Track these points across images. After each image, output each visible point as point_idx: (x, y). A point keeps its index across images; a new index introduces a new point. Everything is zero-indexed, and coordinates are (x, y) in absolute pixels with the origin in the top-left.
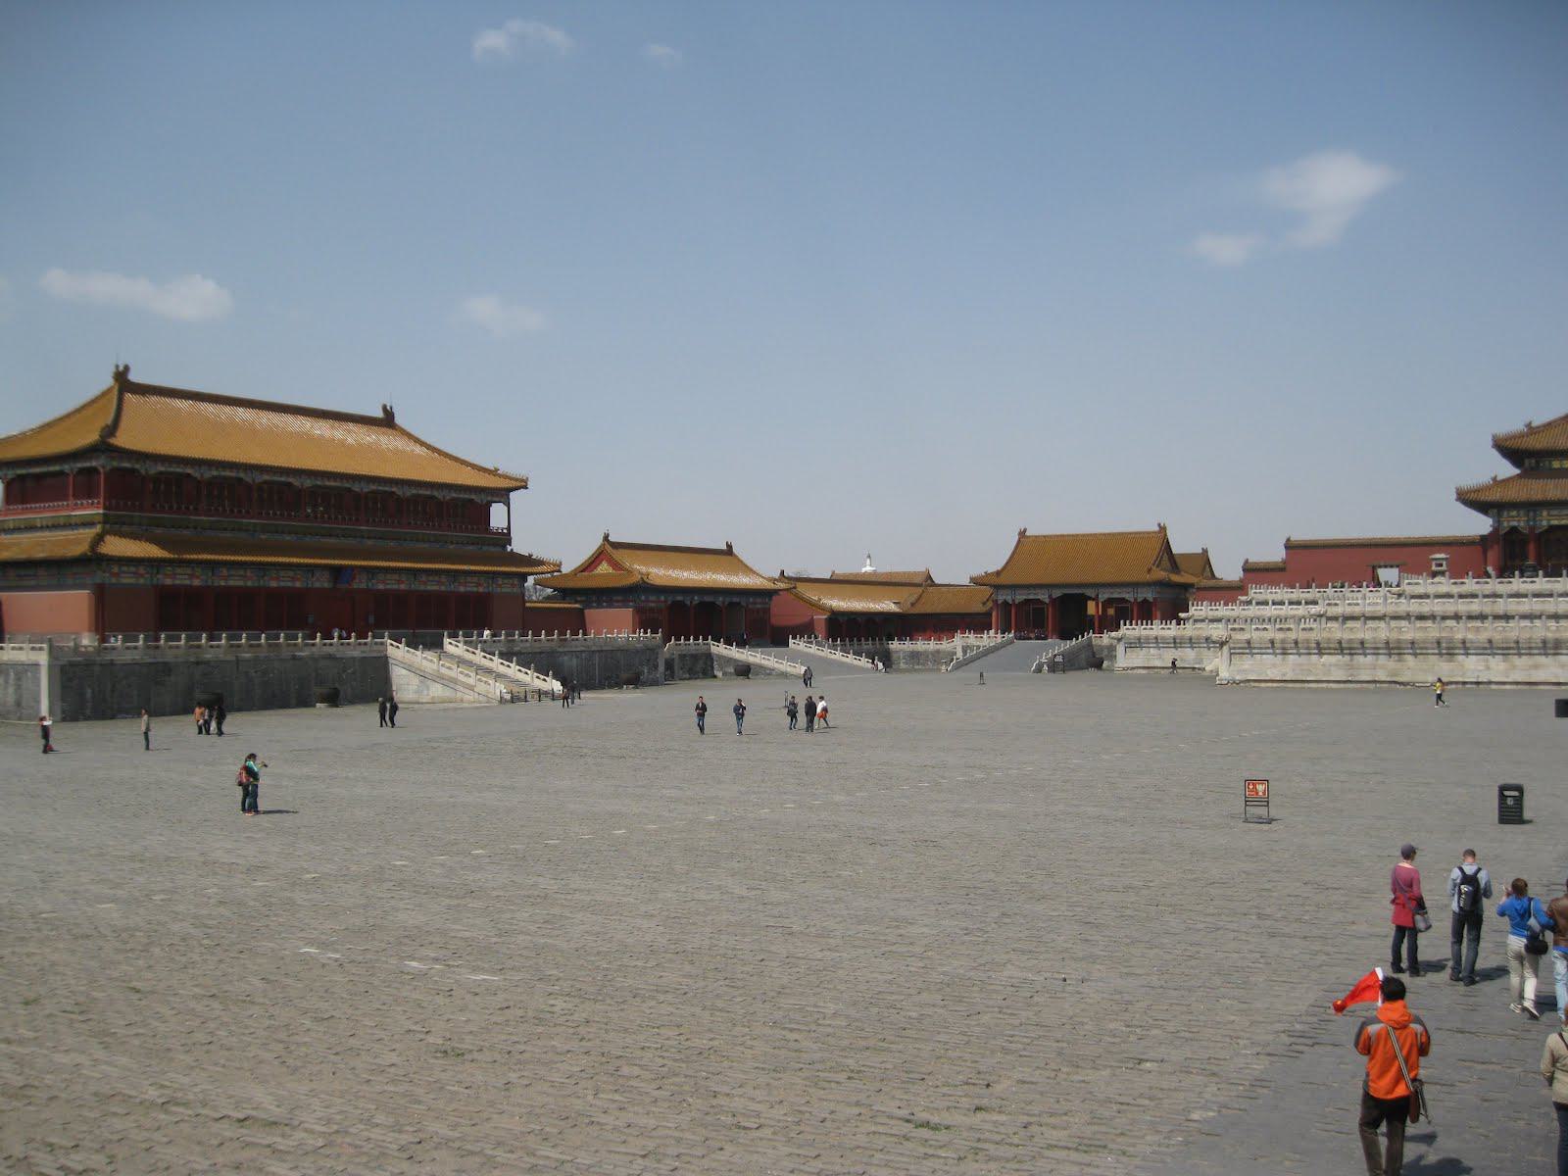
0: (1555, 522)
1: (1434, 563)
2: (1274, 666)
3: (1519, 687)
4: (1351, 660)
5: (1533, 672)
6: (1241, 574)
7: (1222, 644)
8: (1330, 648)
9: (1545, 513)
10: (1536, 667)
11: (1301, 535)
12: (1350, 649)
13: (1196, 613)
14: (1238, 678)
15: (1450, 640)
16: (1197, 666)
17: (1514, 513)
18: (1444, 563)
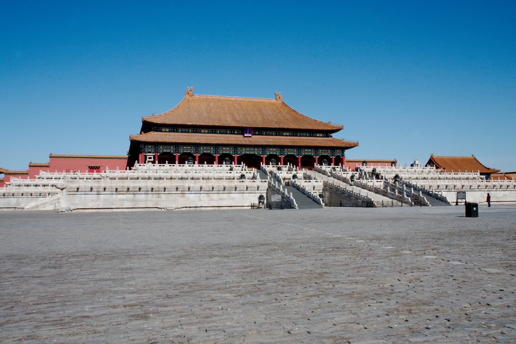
0: (165, 151)
1: (148, 157)
2: (92, 201)
3: (215, 208)
4: (134, 197)
5: (220, 201)
6: (28, 168)
7: (62, 189)
8: (123, 191)
9: (161, 147)
10: (221, 199)
11: (56, 153)
12: (134, 191)
13: (14, 182)
14: (72, 208)
15: (183, 187)
16: (17, 207)
17: (150, 147)
18: (152, 157)
